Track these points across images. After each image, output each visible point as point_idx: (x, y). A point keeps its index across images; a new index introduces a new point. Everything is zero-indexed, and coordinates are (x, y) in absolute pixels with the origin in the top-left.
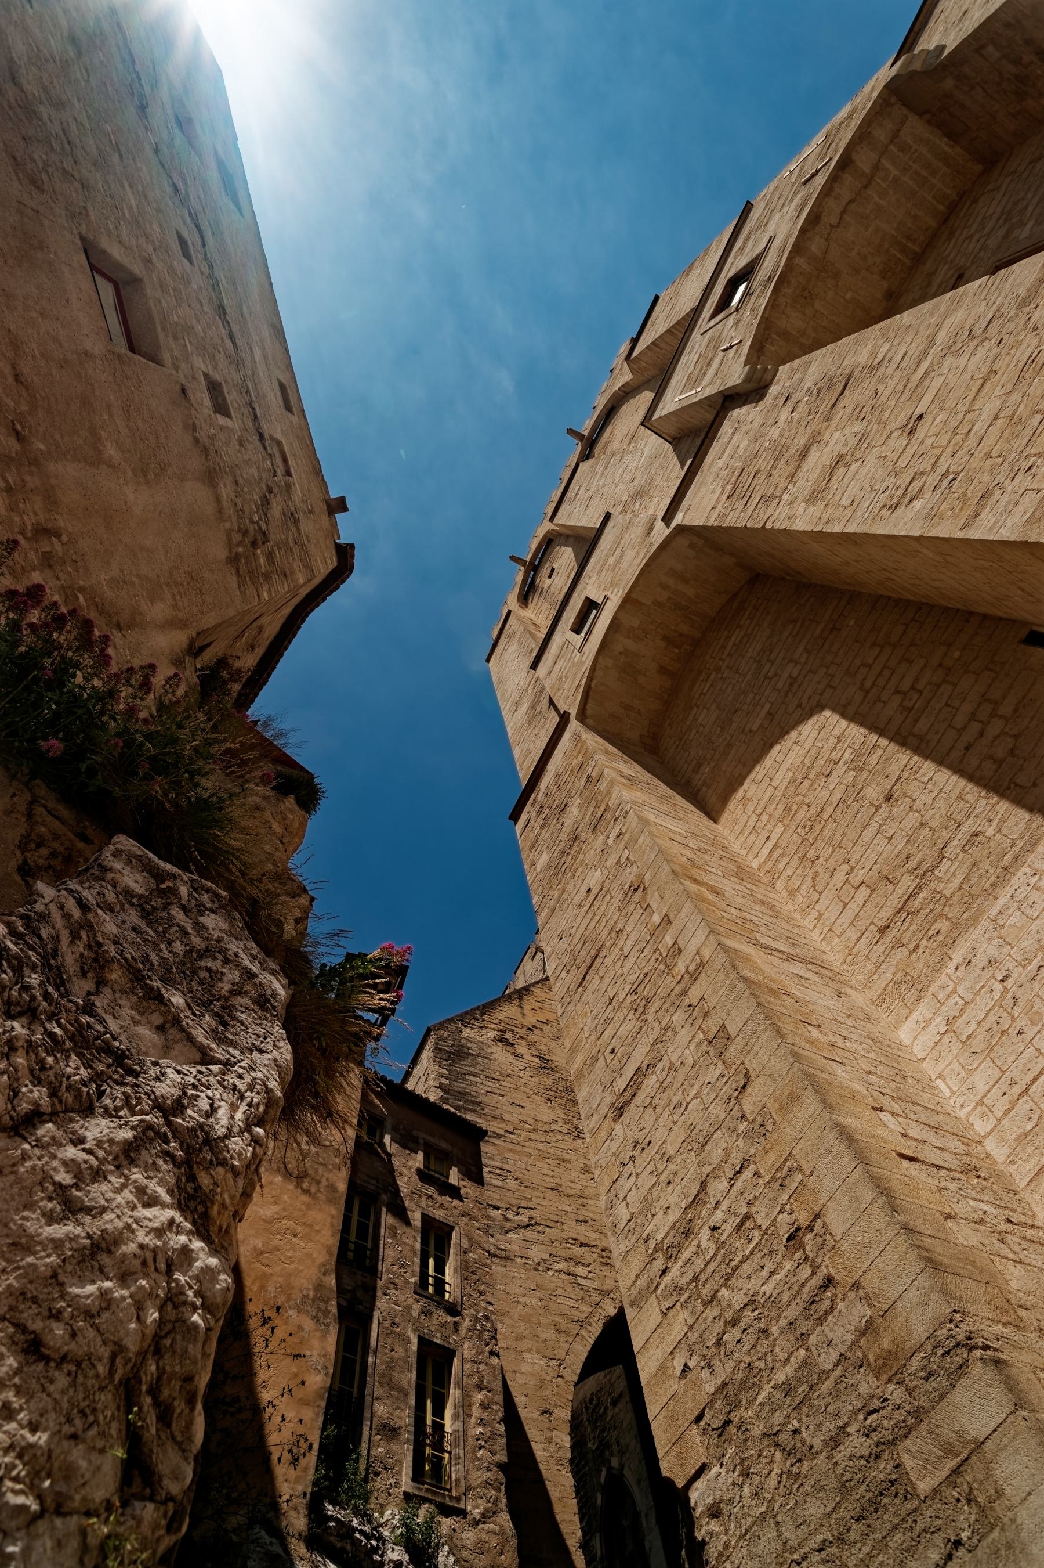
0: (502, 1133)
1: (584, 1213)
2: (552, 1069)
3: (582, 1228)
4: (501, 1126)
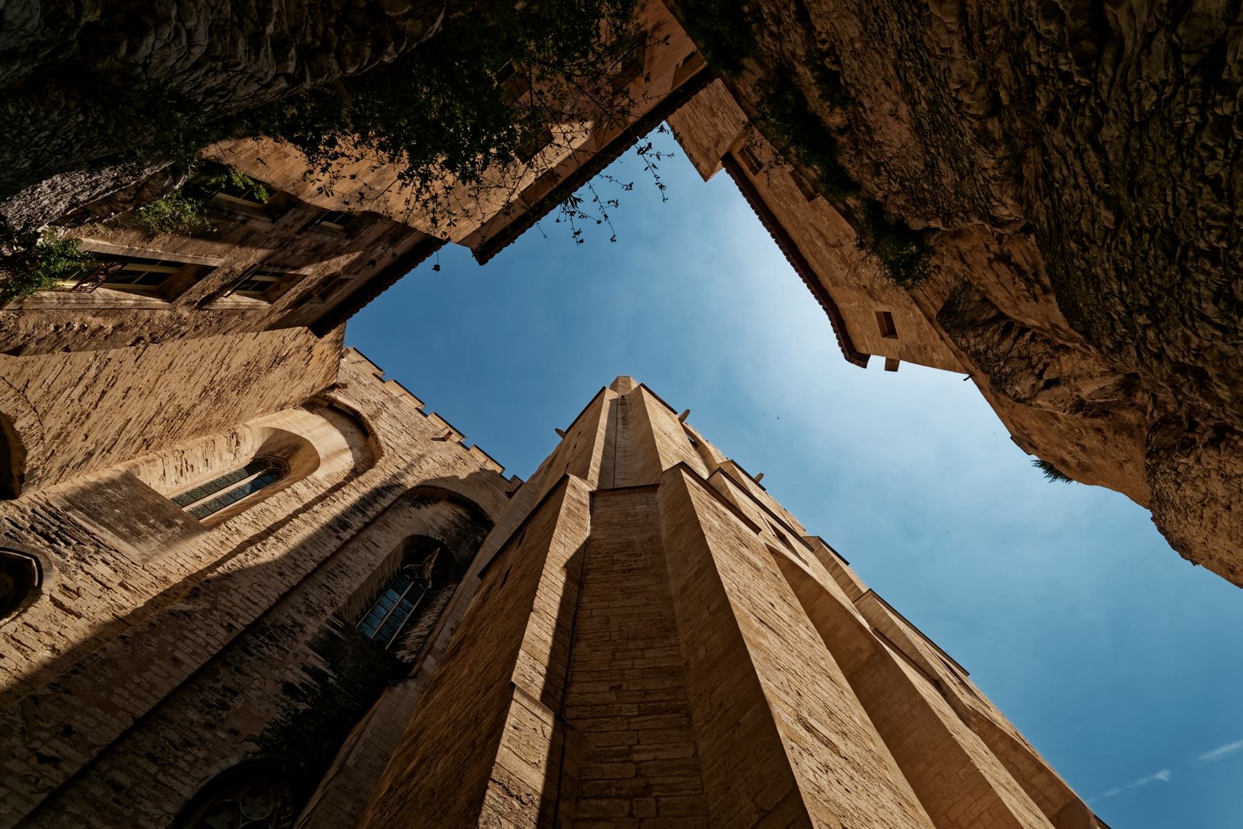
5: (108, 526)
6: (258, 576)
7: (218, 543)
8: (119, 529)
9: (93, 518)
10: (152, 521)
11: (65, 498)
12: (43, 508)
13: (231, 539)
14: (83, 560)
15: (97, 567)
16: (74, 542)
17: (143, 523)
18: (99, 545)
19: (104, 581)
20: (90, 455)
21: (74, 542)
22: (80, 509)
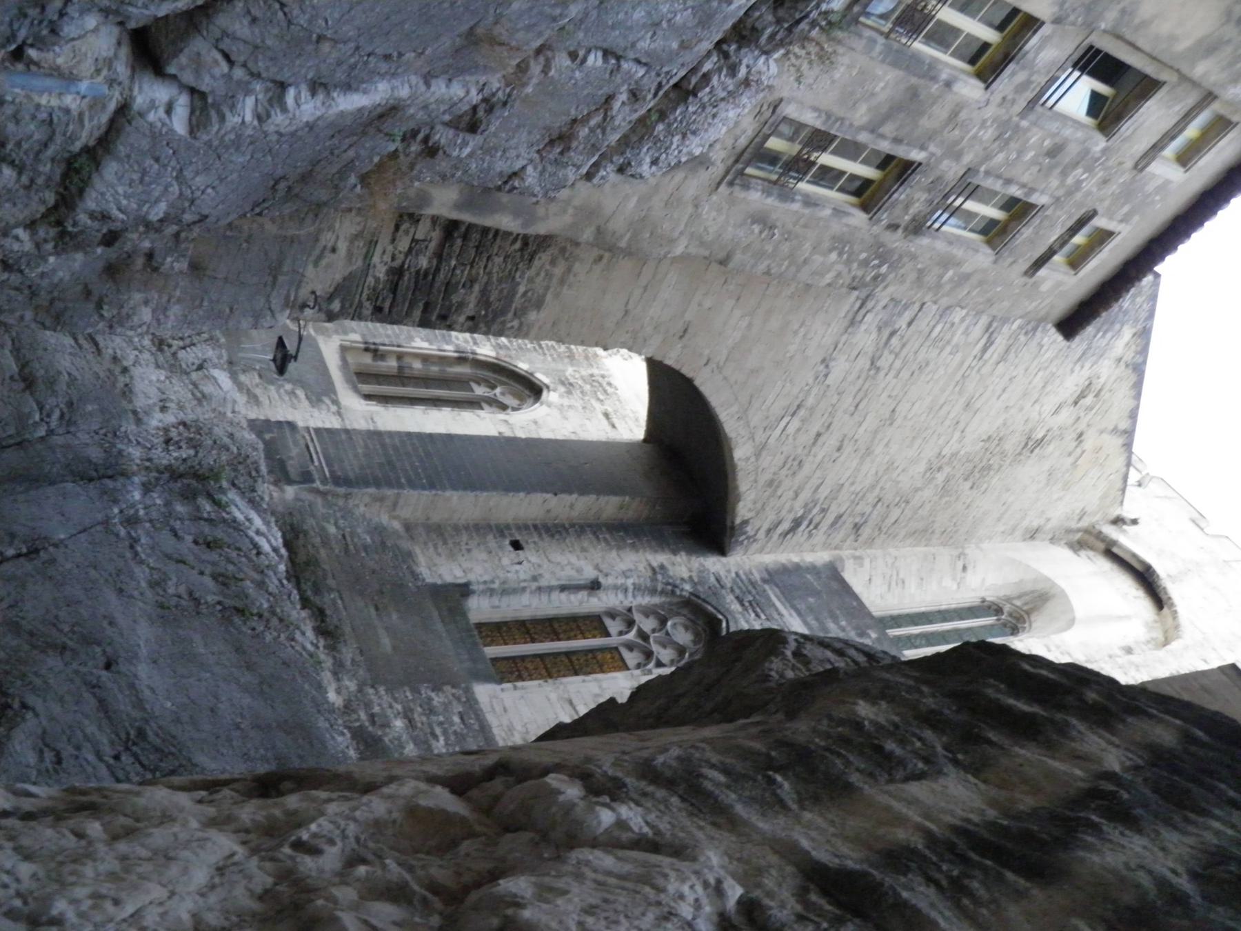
1: (848, 448)
5: (799, 614)
10: (843, 623)
11: (767, 570)
12: (745, 574)
16: (763, 617)
20: (797, 523)
21: (763, 617)
22: (777, 586)
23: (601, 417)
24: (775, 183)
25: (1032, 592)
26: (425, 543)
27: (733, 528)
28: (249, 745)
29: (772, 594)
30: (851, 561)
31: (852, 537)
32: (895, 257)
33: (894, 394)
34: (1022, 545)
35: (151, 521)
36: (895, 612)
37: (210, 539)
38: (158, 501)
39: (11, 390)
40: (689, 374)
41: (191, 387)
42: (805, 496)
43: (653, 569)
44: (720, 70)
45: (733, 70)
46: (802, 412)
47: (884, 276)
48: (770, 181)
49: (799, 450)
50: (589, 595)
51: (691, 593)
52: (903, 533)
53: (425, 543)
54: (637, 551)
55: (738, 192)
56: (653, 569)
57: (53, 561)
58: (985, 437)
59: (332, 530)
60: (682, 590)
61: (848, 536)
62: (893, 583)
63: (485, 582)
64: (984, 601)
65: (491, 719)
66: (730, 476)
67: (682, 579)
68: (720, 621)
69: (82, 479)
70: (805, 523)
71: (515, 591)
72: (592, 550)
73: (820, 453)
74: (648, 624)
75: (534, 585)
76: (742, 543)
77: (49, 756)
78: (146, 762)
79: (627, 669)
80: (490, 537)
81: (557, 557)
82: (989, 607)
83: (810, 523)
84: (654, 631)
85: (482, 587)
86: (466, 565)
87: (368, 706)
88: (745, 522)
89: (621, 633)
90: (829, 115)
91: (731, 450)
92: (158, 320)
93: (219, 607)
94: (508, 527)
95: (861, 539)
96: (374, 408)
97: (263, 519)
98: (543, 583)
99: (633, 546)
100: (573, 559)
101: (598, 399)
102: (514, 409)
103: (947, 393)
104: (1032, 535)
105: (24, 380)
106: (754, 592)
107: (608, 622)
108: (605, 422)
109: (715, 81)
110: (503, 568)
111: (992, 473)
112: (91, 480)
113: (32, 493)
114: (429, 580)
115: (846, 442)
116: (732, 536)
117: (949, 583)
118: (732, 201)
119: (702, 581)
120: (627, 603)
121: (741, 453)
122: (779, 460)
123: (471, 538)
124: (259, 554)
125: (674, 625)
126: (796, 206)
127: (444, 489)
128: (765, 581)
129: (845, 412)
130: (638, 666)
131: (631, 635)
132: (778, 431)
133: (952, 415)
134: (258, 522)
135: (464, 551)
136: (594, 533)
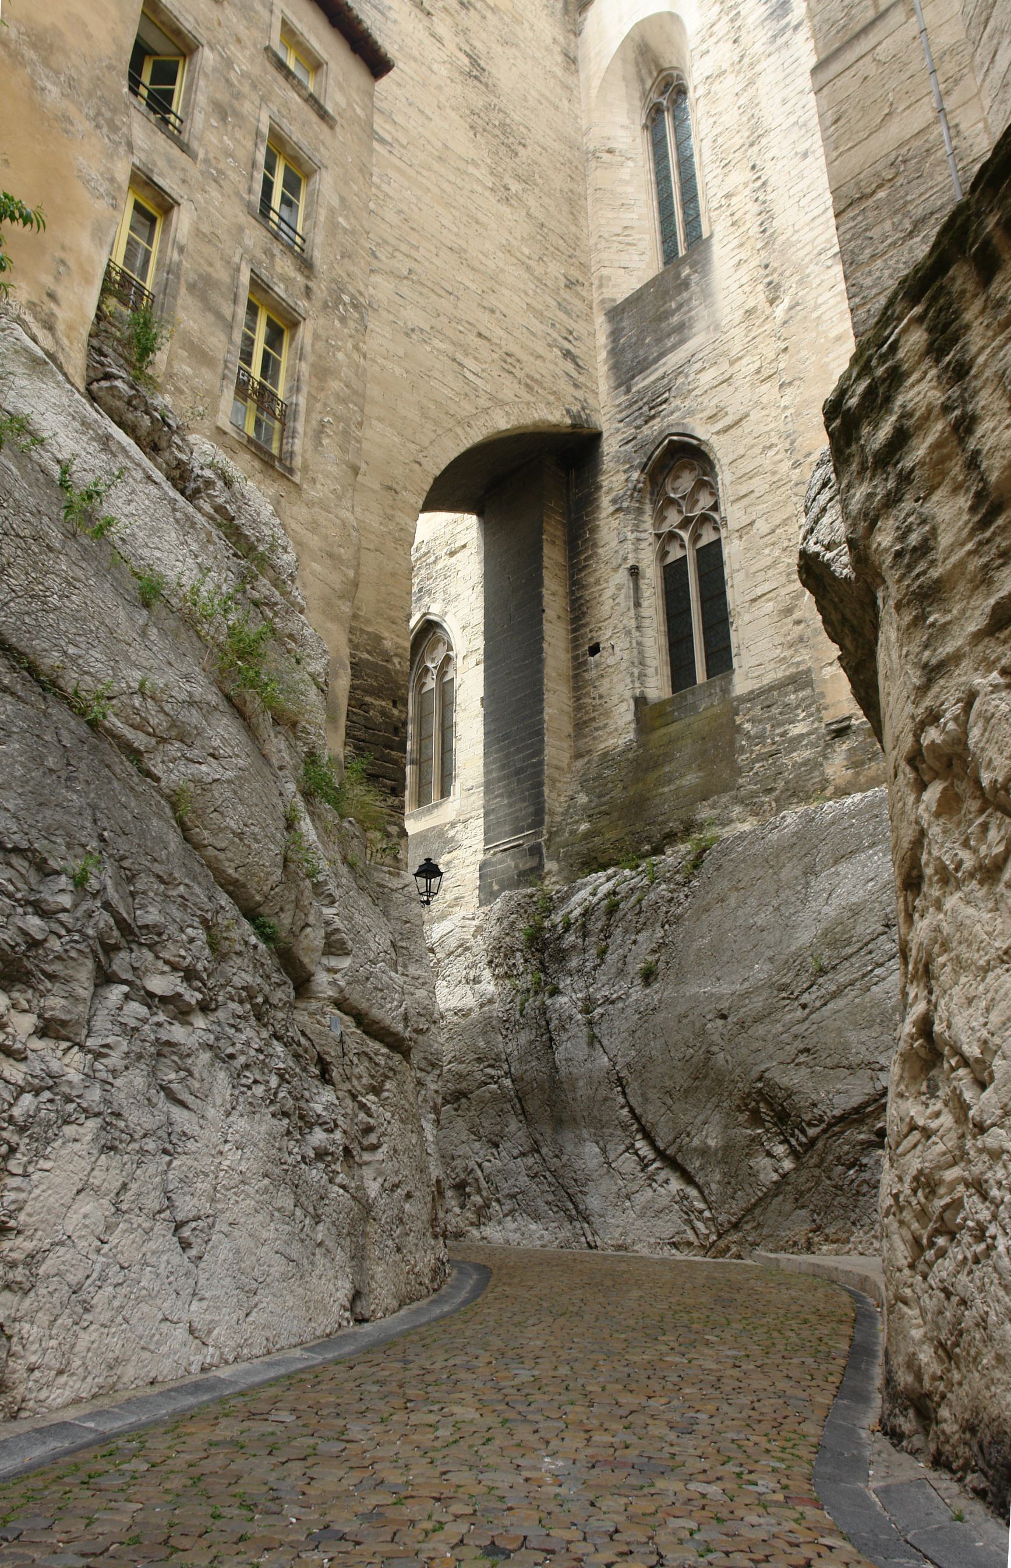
0: (389, 139)
1: (491, 300)
2: (487, 85)
3: (486, 317)
4: (387, 126)
6: (792, 192)
7: (732, 229)
8: (669, 344)
9: (647, 368)
10: (673, 305)
11: (616, 388)
12: (621, 412)
13: (735, 209)
14: (690, 391)
15: (702, 382)
16: (666, 395)
17: (673, 315)
18: (679, 371)
19: (721, 379)
20: (567, 354)
21: (666, 395)
22: (633, 377)
23: (453, 560)
24: (284, 424)
25: (637, 64)
26: (594, 738)
27: (573, 426)
28: (793, 899)
29: (641, 383)
30: (604, 290)
31: (579, 288)
32: (334, 286)
33: (435, 251)
34: (582, 76)
35: (587, 987)
36: (659, 237)
37: (602, 936)
38: (568, 982)
39: (468, 1109)
40: (431, 481)
41: (452, 958)
42: (540, 348)
43: (617, 510)
44: (209, 496)
45: (209, 483)
46: (459, 357)
47: (353, 297)
48: (283, 430)
49: (495, 356)
50: (644, 578)
51: (642, 471)
52: (573, 229)
53: (594, 738)
54: (598, 526)
55: (298, 462)
56: (617, 510)
57: (628, 1065)
58: (471, 134)
59: (584, 827)
60: (638, 481)
61: (577, 295)
62: (628, 240)
63: (633, 682)
64: (645, 127)
65: (766, 681)
66: (522, 431)
67: (627, 480)
68: (671, 441)
69: (551, 1047)
70: (567, 345)
71: (641, 653)
72: (598, 574)
73: (497, 333)
74: (673, 518)
75: (635, 633)
76: (588, 415)
77: (802, 1058)
78: (808, 984)
79: (718, 543)
80: (587, 676)
81: (606, 608)
82: (654, 120)
83: (566, 339)
84: (680, 512)
85: (637, 685)
86: (615, 699)
87: (754, 794)
88: (568, 411)
89: (683, 546)
90: (224, 377)
91: (500, 432)
92: (424, 984)
93: (667, 927)
94: (575, 658)
95: (581, 279)
96: (457, 788)
97: (579, 890)
98: (633, 623)
99: (594, 530)
100: (608, 593)
101: (435, 562)
102: (450, 648)
103: (428, 184)
104: (571, 61)
105: (458, 1099)
106: (641, 403)
107: (670, 559)
108: (458, 556)
109: (220, 501)
110: (618, 663)
111: (508, 121)
112: (551, 1039)
113: (565, 1086)
114: (631, 736)
115: (485, 304)
116: (582, 427)
117: (625, 173)
118: (305, 468)
119: (628, 460)
120: (651, 539)
121: (502, 422)
122: (507, 380)
123: (588, 694)
124: (615, 893)
125: (675, 490)
126: (302, 400)
127: (541, 722)
128: (628, 391)
129: (456, 307)
130: (716, 529)
131: (685, 535)
132: (479, 382)
133: (452, 178)
134: (583, 894)
135: (602, 701)
136: (580, 570)
